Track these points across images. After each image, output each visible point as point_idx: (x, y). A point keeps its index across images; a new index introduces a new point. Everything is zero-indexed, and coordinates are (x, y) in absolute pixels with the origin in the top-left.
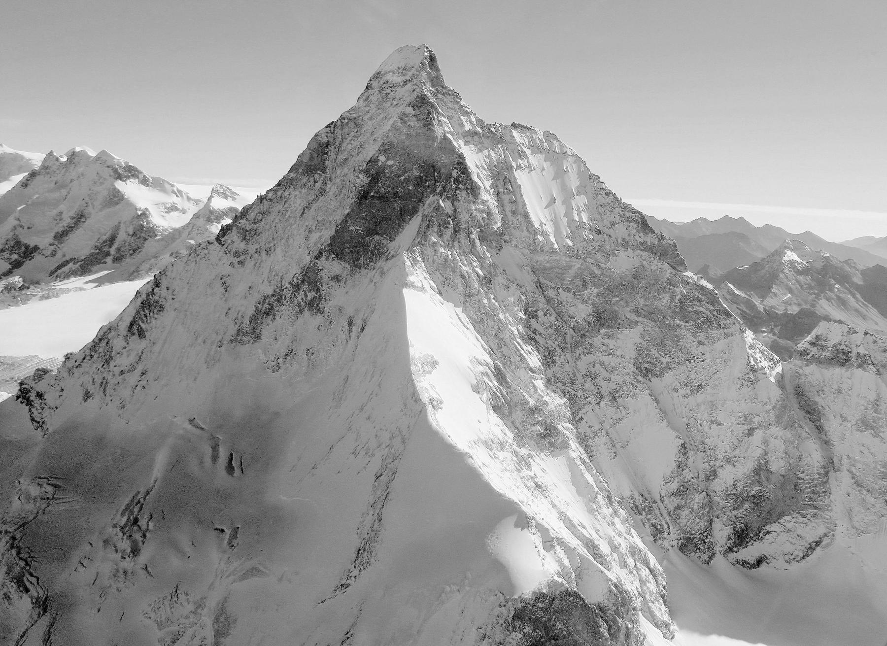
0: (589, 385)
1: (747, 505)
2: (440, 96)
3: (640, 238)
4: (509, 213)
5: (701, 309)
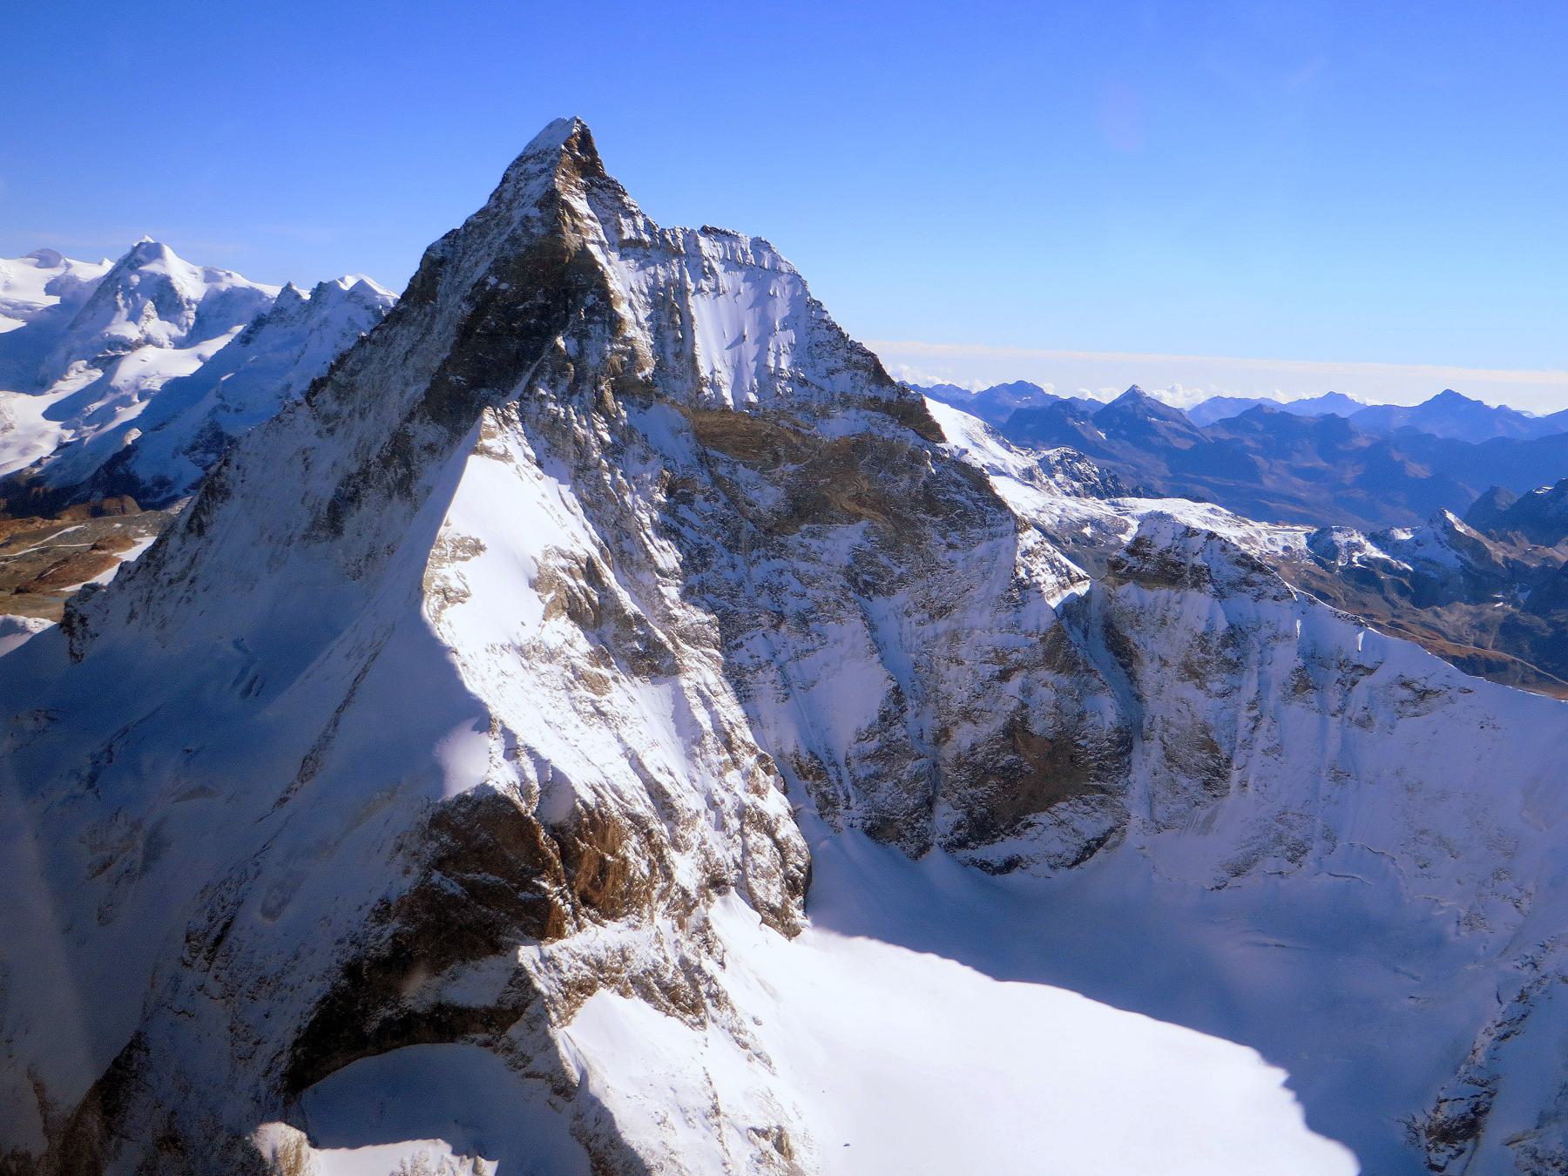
0: (764, 600)
1: (992, 782)
2: (595, 190)
3: (870, 391)
4: (670, 357)
5: (958, 497)
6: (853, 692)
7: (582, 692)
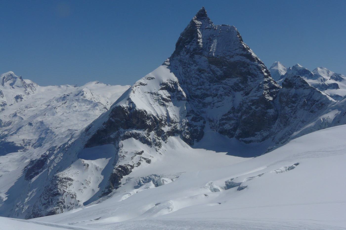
7: (162, 101)
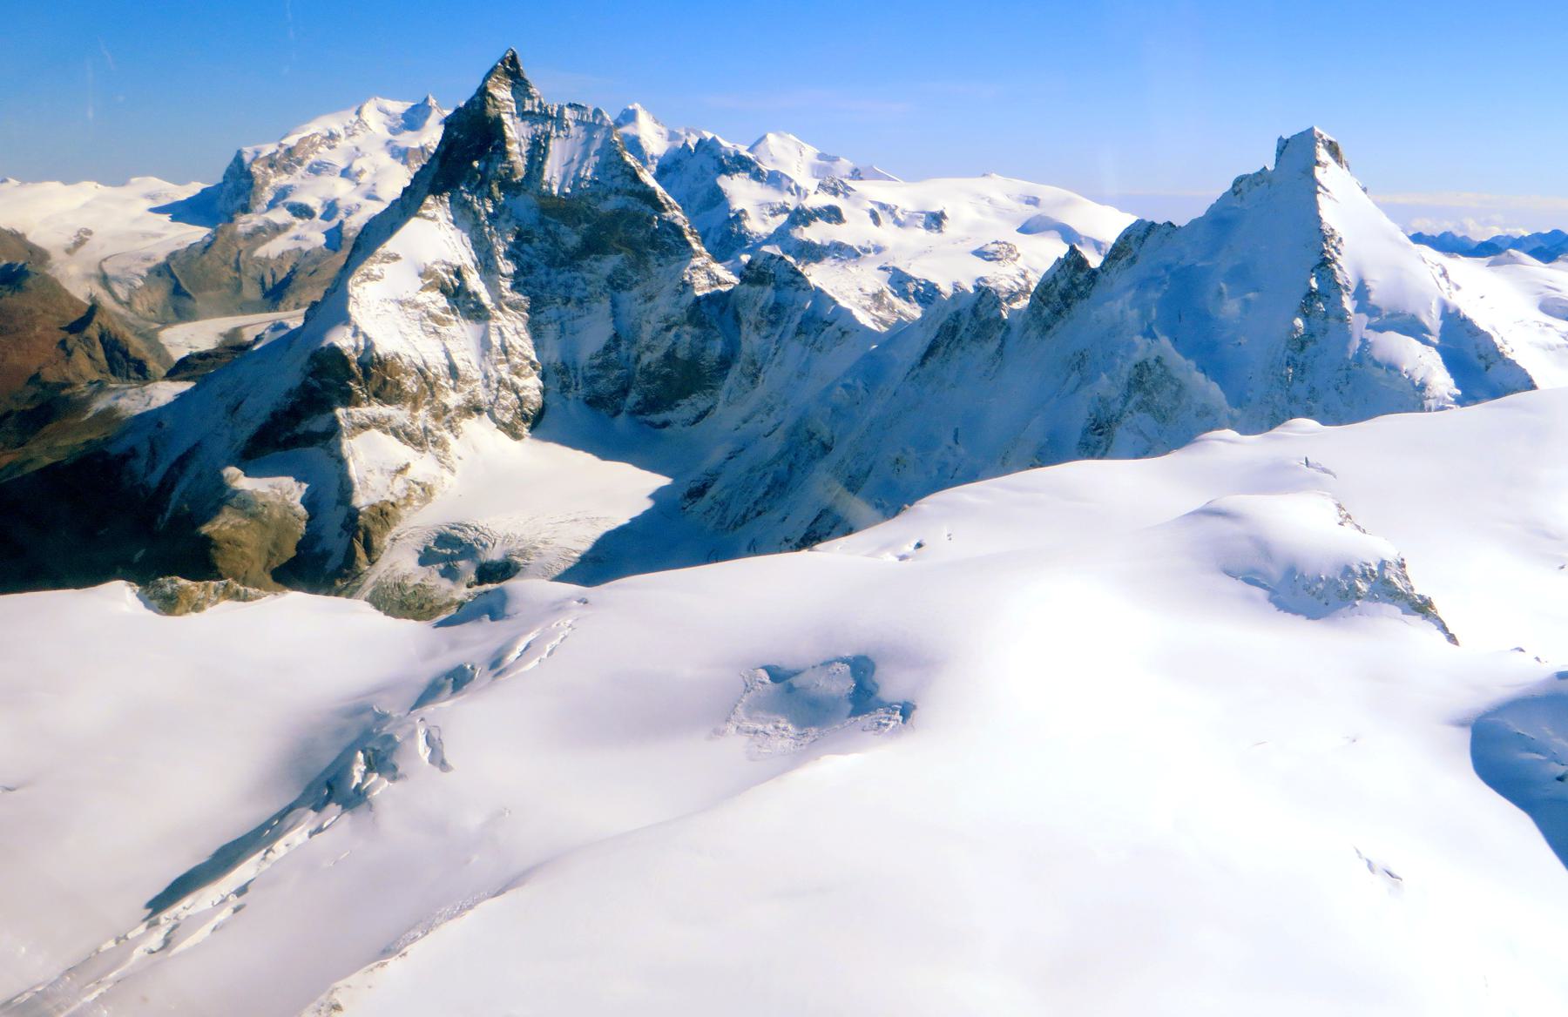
0: (561, 291)
6: (594, 333)
7: (429, 322)
